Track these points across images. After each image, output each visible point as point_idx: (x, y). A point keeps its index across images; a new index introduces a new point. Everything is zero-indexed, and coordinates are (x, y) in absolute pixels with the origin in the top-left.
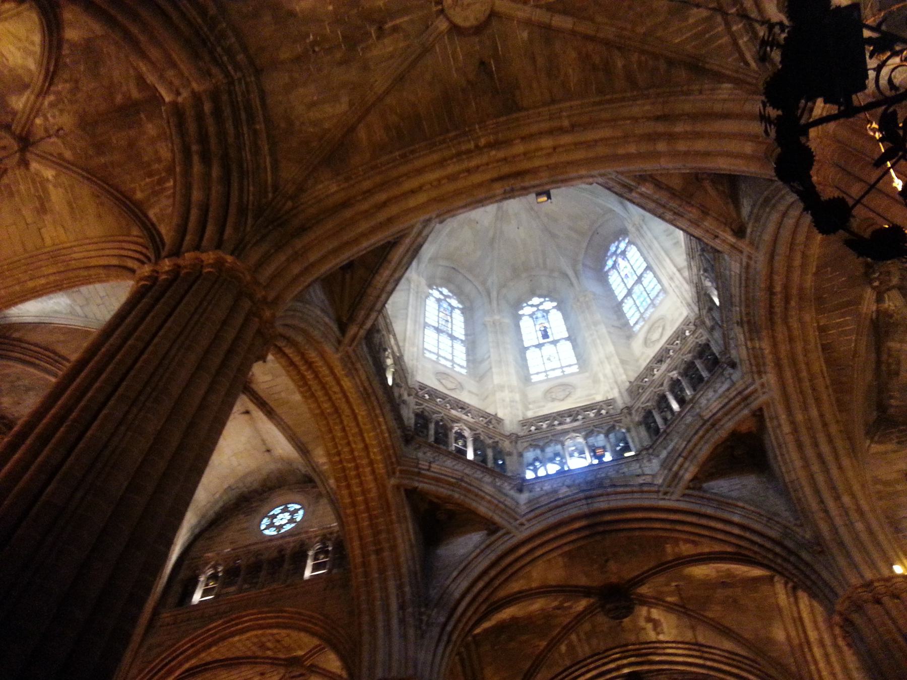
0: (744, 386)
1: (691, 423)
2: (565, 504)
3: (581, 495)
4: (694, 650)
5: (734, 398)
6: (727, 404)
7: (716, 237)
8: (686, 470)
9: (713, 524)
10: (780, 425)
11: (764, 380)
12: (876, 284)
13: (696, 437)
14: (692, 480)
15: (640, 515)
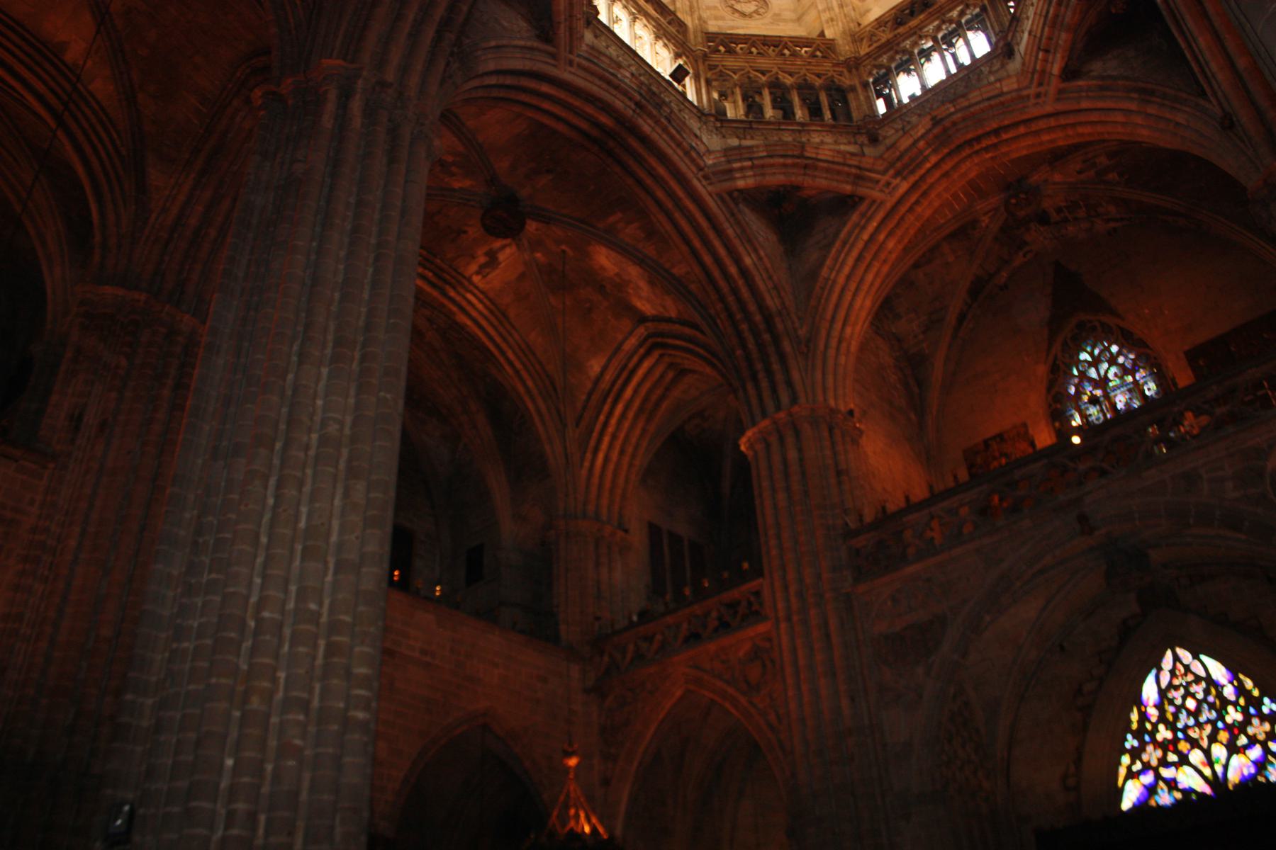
0: (868, 166)
1: (786, 144)
2: (617, 88)
3: (638, 97)
4: (496, 317)
5: (850, 166)
6: (838, 163)
7: (1047, 51)
8: (744, 177)
9: (717, 243)
10: (864, 228)
11: (895, 182)
12: (1013, 201)
13: (781, 160)
14: (740, 191)
15: (661, 170)
